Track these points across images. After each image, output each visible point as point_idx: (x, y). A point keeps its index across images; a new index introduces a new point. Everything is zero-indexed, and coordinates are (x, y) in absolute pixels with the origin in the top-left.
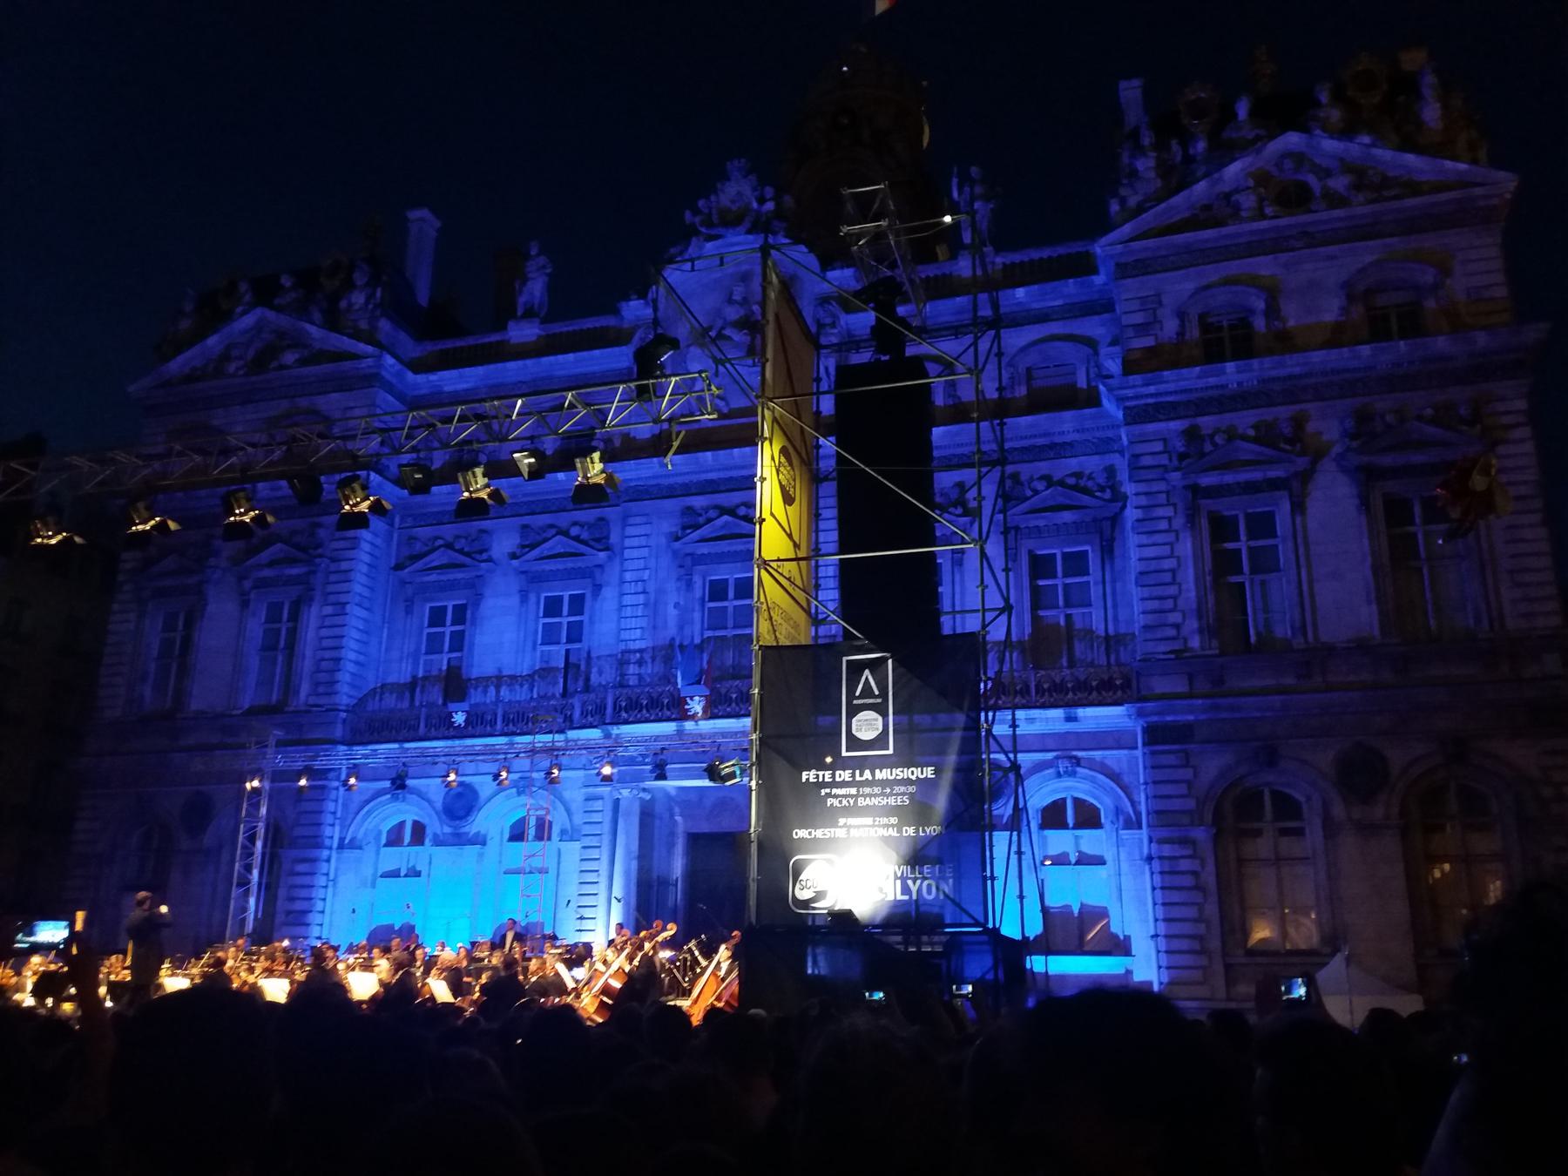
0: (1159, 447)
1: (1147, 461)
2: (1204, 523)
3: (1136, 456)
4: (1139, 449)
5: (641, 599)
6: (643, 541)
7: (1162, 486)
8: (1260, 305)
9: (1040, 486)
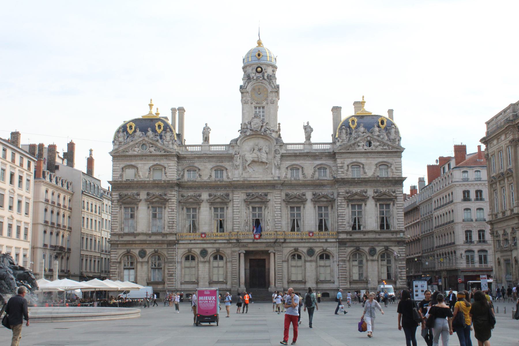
0: (343, 191)
1: (341, 193)
2: (350, 206)
3: (339, 192)
4: (340, 191)
5: (238, 211)
6: (238, 198)
7: (343, 198)
8: (362, 166)
9: (320, 194)
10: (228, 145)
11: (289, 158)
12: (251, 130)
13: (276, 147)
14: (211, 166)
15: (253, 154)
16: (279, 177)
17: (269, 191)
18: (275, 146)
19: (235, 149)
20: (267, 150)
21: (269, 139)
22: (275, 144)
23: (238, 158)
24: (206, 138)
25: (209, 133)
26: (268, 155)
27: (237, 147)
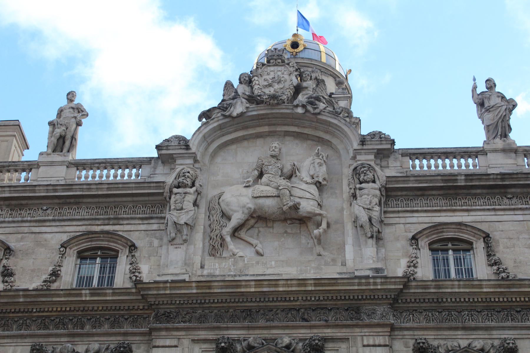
10: (149, 160)
11: (419, 204)
12: (252, 99)
13: (358, 157)
14: (65, 237)
15: (257, 186)
16: (377, 270)
17: (328, 332)
18: (354, 158)
19: (179, 168)
20: (321, 172)
21: (327, 137)
22: (356, 145)
23: (191, 198)
24: (62, 139)
25: (79, 124)
26: (325, 195)
27: (190, 161)
